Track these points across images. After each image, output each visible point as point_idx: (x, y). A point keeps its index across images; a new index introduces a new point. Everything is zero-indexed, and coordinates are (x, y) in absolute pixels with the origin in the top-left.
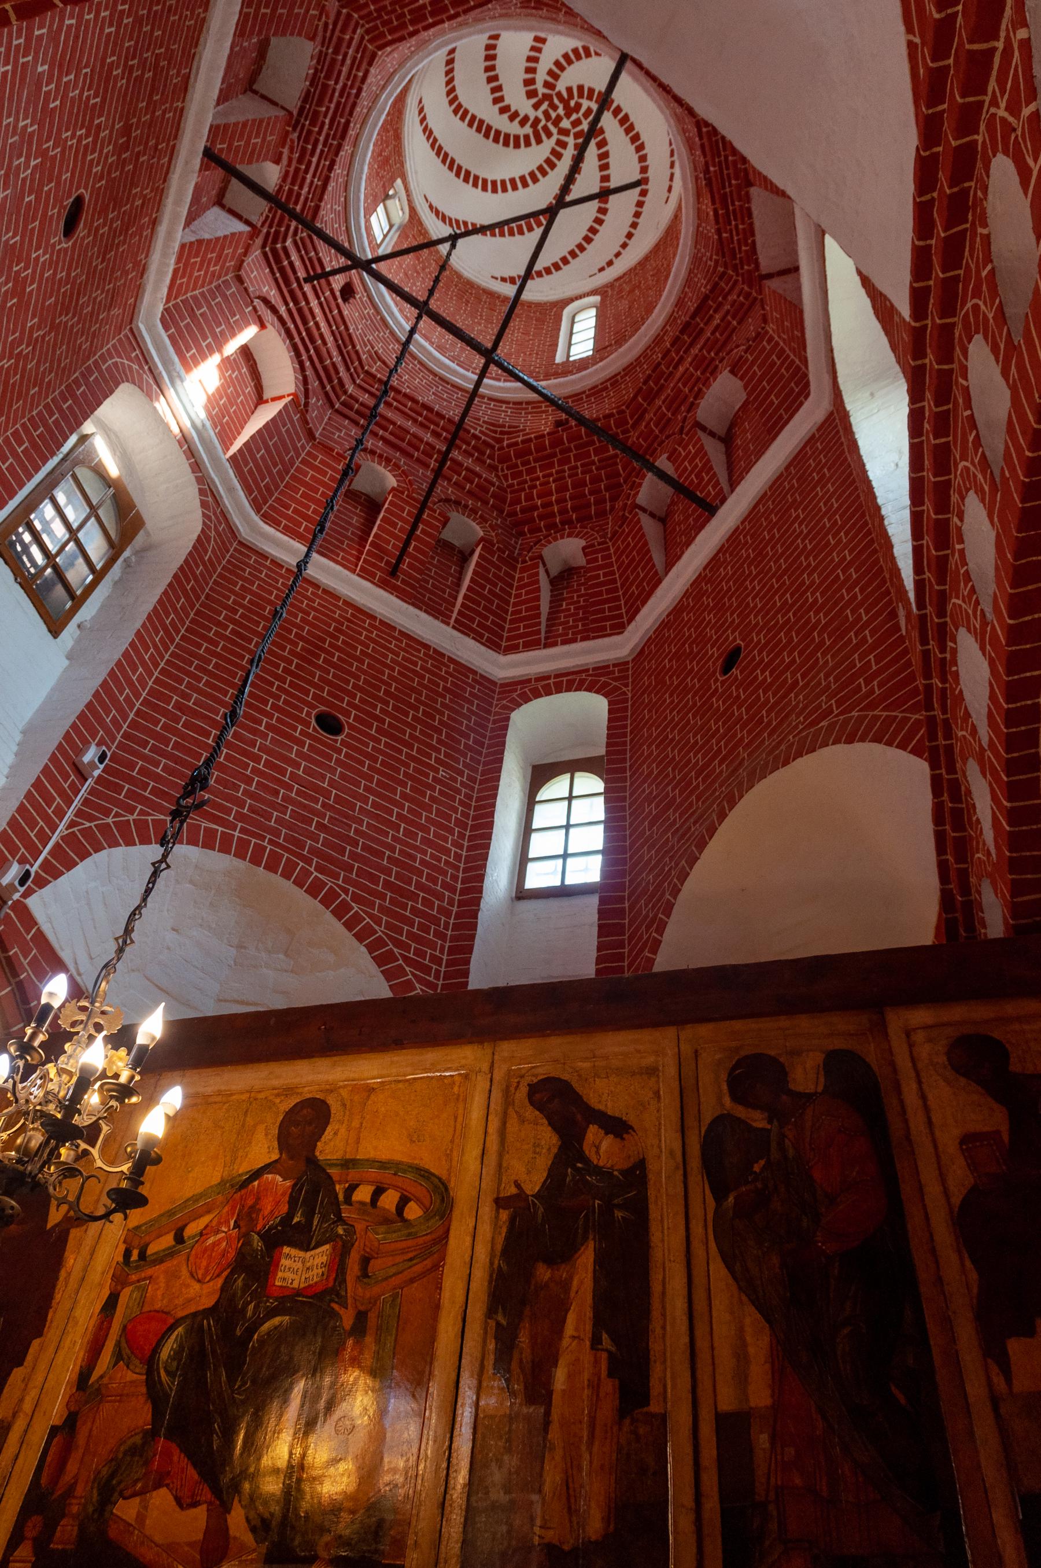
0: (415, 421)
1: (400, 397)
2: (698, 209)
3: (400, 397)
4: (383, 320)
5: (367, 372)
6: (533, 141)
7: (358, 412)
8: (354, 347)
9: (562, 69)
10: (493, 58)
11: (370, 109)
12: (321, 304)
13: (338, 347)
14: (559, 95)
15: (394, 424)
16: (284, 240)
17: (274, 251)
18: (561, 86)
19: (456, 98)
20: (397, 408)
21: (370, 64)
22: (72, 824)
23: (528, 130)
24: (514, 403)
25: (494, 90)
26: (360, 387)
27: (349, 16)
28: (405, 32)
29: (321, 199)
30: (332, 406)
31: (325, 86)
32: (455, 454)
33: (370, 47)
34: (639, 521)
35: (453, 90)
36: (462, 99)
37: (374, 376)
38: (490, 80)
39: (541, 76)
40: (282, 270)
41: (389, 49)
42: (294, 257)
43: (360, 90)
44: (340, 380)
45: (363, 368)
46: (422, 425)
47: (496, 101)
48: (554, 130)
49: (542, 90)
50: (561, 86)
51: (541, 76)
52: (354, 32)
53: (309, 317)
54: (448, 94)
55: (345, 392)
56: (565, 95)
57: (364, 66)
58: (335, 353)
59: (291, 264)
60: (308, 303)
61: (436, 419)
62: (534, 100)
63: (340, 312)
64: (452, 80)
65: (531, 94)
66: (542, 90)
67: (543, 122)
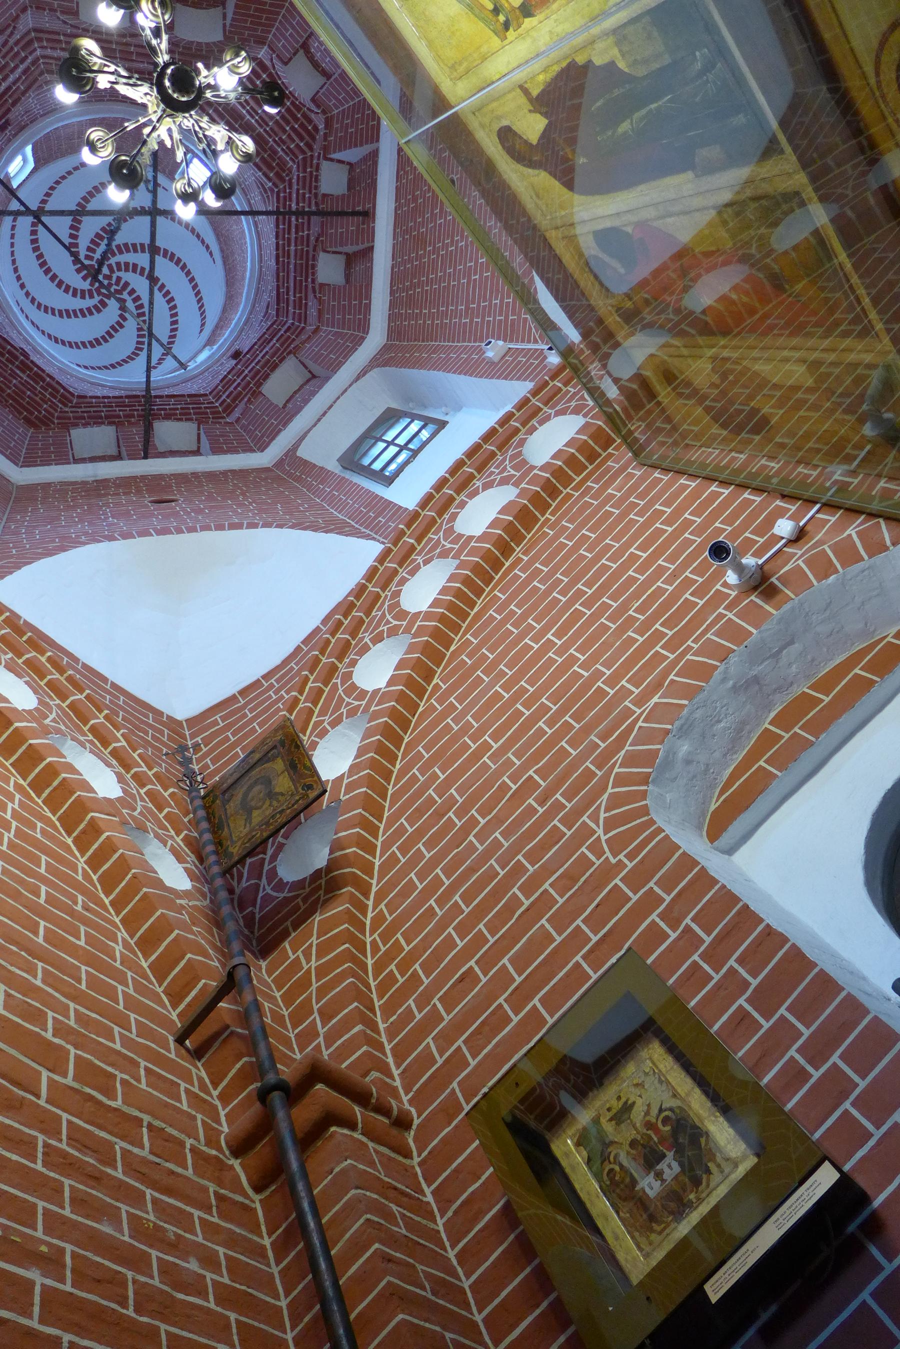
0: (288, 263)
1: (281, 283)
2: (31, 122)
3: (281, 283)
4: (245, 323)
5: (277, 316)
6: (129, 289)
7: (300, 309)
8: (265, 333)
9: (75, 291)
10: (96, 340)
11: (121, 389)
12: (246, 368)
13: (268, 343)
14: (92, 284)
15: (295, 277)
16: (217, 407)
17: (224, 411)
18: (86, 285)
19: (133, 353)
20: (288, 282)
21: (85, 397)
22: (536, 341)
23: (125, 295)
24: (246, 195)
25: (116, 331)
26: (287, 317)
27: (58, 418)
28: (54, 383)
29: (183, 396)
30: (303, 328)
31: (107, 417)
32: (293, 219)
33: (75, 401)
34: (231, 25)
35: (129, 357)
36: (132, 349)
37: (278, 310)
38: (111, 336)
39: (89, 303)
40: (234, 400)
41: (71, 390)
42: (224, 397)
43: (104, 397)
44: (285, 332)
45: (276, 321)
46: (289, 257)
47: (122, 326)
48: (114, 276)
49: (97, 298)
50: (86, 285)
51: (89, 303)
52: (67, 412)
53: (255, 370)
54: (133, 359)
55: (293, 324)
56: (89, 280)
57: (89, 400)
58: (272, 344)
59: (228, 397)
60: (247, 375)
61: (281, 249)
62: (106, 300)
63: (247, 353)
64: (124, 361)
65: (105, 305)
66: (97, 298)
67: (114, 287)
